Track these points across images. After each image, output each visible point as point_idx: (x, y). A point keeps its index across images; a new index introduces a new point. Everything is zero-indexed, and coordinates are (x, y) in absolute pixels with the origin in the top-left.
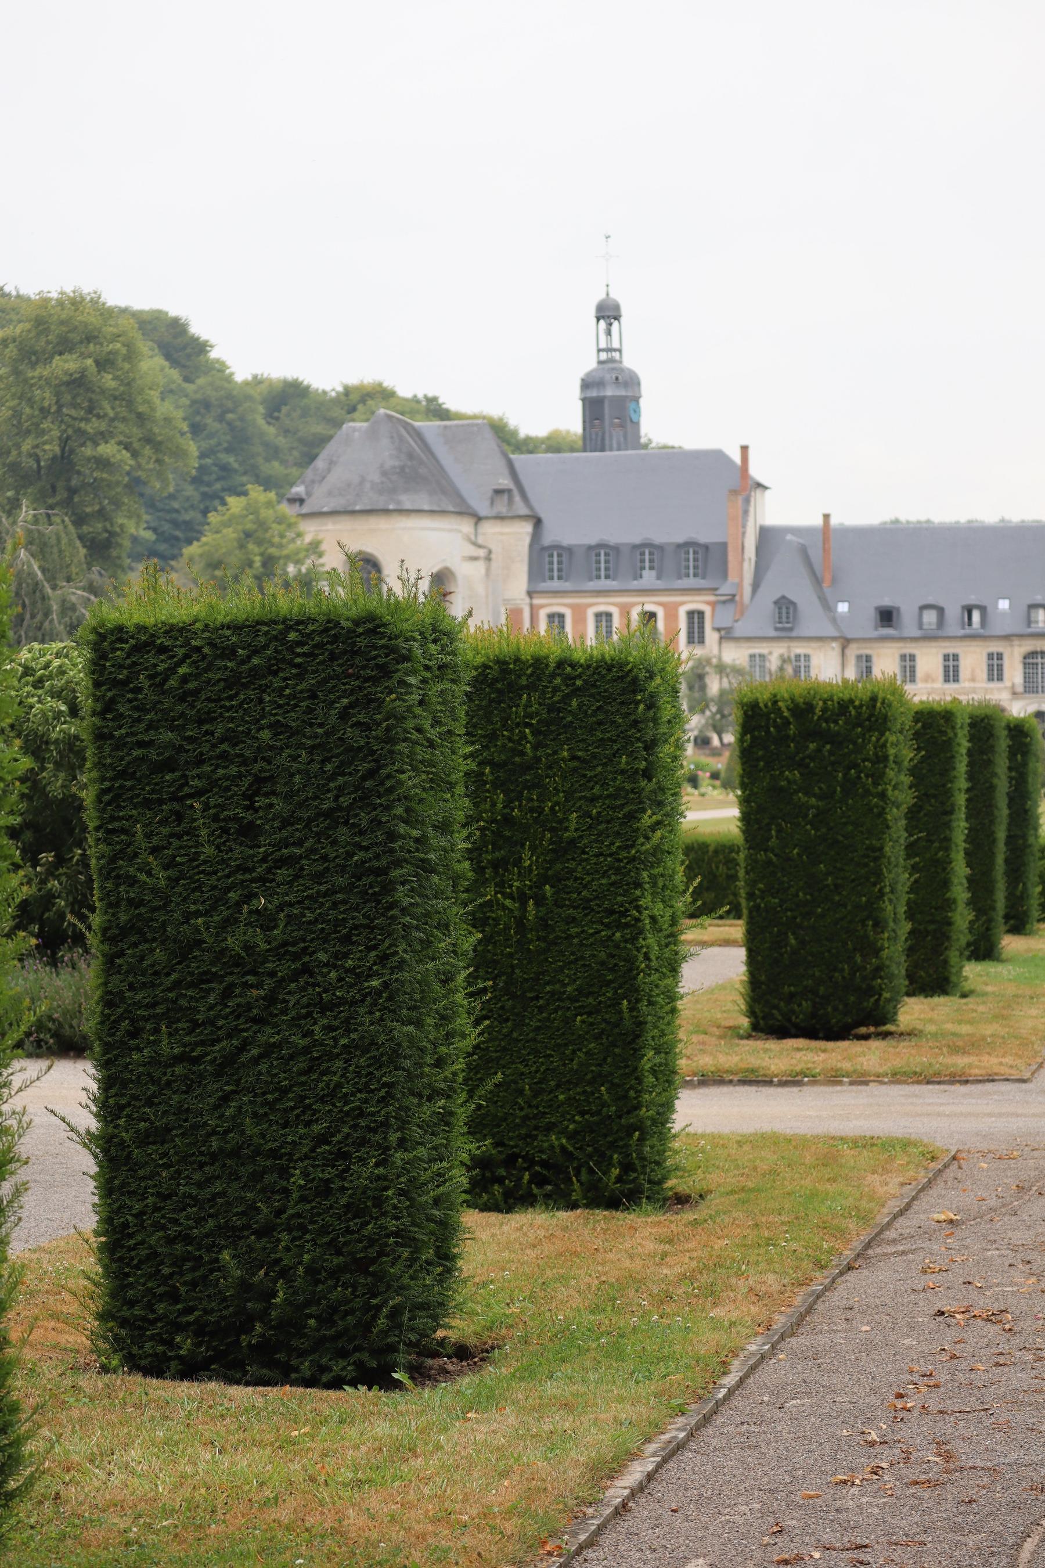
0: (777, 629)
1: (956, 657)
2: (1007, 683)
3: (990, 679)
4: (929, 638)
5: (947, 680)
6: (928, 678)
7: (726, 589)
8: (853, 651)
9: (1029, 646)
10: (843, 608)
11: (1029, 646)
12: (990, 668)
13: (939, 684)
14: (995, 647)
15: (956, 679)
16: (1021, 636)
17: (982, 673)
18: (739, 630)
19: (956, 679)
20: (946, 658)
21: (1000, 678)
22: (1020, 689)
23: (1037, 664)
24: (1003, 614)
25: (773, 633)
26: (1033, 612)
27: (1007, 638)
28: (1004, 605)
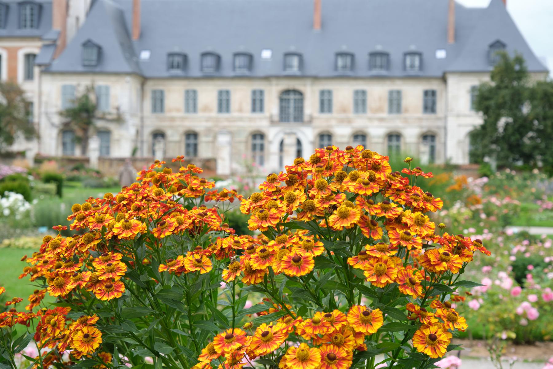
0: (84, 66)
1: (228, 92)
2: (267, 113)
3: (254, 110)
4: (207, 78)
5: (220, 110)
6: (206, 109)
7: (51, 35)
8: (150, 86)
9: (285, 85)
10: (145, 55)
11: (285, 85)
12: (254, 101)
13: (214, 113)
14: (258, 86)
15: (228, 110)
16: (278, 77)
17: (248, 105)
18: (56, 65)
19: (228, 110)
20: (220, 93)
21: (261, 109)
22: (276, 118)
23: (289, 100)
24: (266, 60)
25: (80, 69)
26: (289, 59)
27: (267, 78)
28: (266, 54)
